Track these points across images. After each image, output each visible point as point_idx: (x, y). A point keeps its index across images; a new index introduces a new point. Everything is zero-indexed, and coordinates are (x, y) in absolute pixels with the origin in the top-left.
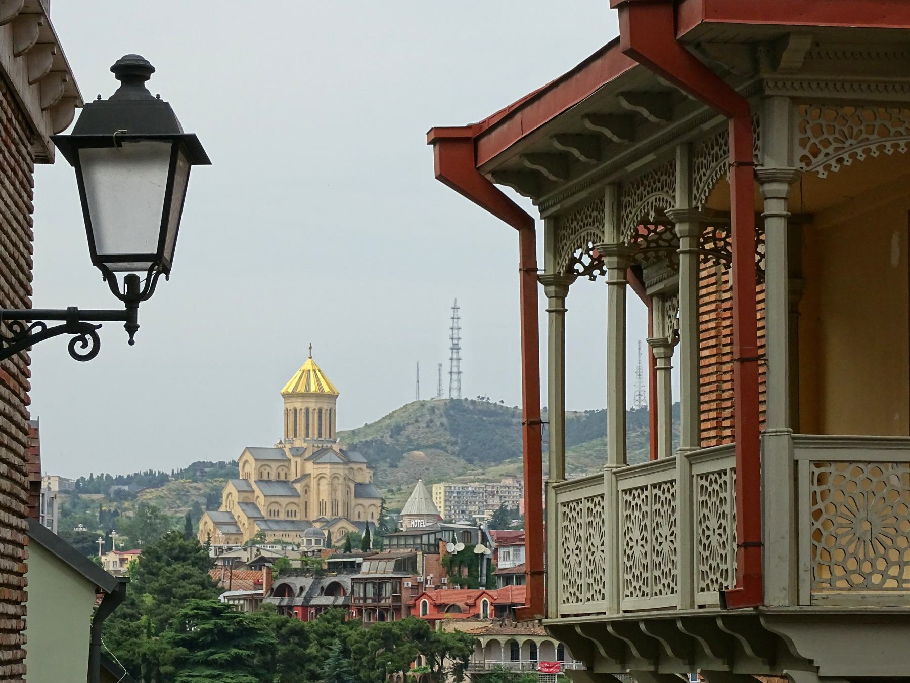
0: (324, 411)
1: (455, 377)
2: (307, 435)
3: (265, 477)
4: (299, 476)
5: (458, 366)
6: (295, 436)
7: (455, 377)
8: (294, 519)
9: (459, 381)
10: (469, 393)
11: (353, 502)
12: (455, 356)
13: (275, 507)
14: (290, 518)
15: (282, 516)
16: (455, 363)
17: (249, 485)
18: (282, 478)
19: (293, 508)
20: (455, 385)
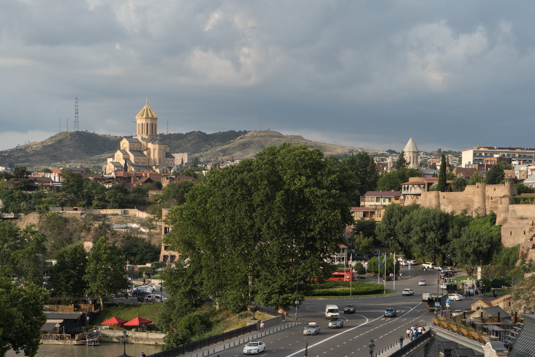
0: (154, 125)
1: (76, 123)
2: (147, 133)
3: (132, 149)
4: (145, 149)
5: (78, 119)
6: (142, 133)
7: (76, 123)
8: (144, 165)
9: (78, 125)
10: (82, 129)
11: (165, 159)
12: (76, 116)
13: (138, 161)
14: (143, 165)
15: (140, 164)
16: (76, 118)
17: (127, 152)
18: (138, 149)
19: (144, 161)
20: (76, 126)
